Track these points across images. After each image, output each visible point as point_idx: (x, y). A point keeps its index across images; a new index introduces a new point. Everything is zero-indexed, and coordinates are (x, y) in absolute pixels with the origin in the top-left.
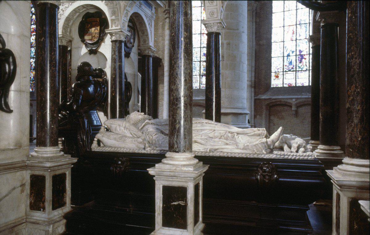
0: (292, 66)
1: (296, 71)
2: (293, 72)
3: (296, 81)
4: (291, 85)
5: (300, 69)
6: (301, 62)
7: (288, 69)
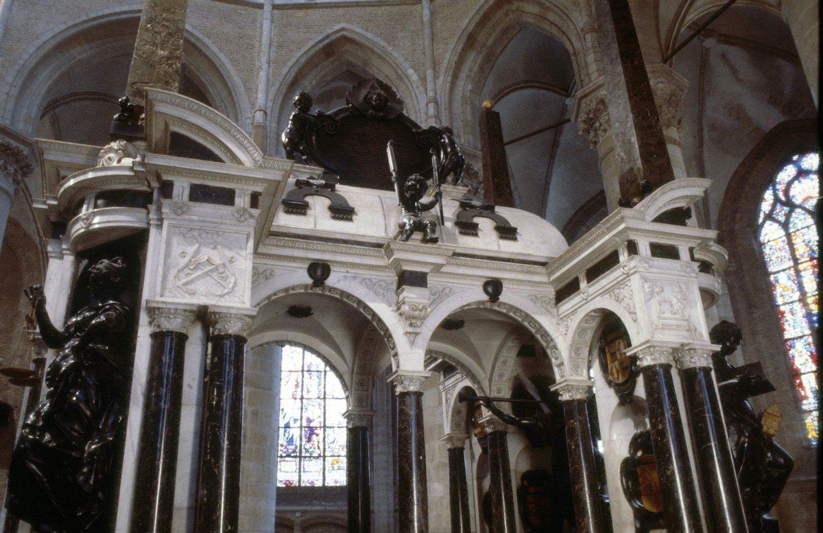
0: (293, 447)
1: (300, 457)
2: (294, 459)
3: (300, 476)
5: (308, 455)
6: (309, 440)
7: (285, 452)
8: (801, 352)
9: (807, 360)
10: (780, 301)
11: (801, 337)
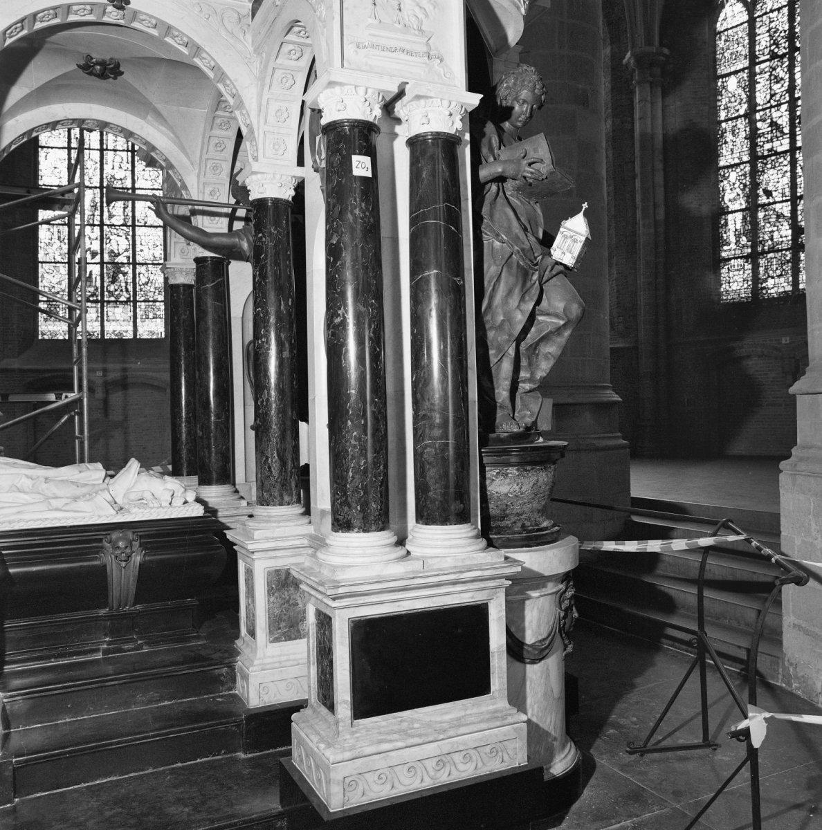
0: (92, 289)
1: (102, 302)
3: (102, 326)
4: (90, 335)
5: (112, 299)
8: (734, 184)
9: (738, 195)
11: (737, 165)
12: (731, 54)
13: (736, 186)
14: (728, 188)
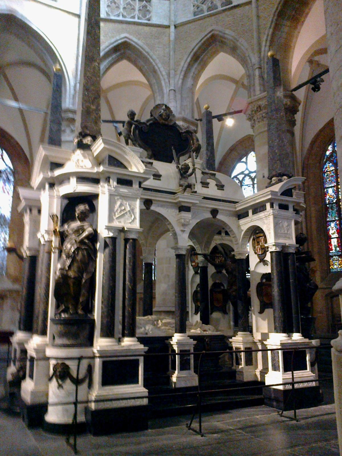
10: (327, 202)
11: (334, 221)
12: (329, 180)
13: (334, 228)
14: (331, 229)
